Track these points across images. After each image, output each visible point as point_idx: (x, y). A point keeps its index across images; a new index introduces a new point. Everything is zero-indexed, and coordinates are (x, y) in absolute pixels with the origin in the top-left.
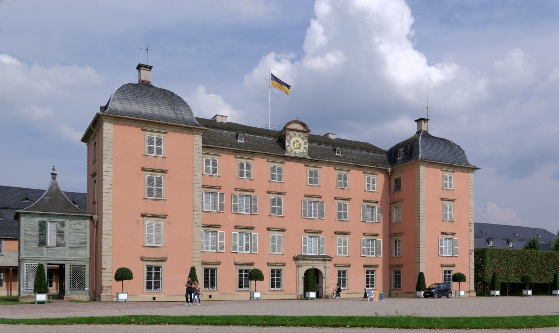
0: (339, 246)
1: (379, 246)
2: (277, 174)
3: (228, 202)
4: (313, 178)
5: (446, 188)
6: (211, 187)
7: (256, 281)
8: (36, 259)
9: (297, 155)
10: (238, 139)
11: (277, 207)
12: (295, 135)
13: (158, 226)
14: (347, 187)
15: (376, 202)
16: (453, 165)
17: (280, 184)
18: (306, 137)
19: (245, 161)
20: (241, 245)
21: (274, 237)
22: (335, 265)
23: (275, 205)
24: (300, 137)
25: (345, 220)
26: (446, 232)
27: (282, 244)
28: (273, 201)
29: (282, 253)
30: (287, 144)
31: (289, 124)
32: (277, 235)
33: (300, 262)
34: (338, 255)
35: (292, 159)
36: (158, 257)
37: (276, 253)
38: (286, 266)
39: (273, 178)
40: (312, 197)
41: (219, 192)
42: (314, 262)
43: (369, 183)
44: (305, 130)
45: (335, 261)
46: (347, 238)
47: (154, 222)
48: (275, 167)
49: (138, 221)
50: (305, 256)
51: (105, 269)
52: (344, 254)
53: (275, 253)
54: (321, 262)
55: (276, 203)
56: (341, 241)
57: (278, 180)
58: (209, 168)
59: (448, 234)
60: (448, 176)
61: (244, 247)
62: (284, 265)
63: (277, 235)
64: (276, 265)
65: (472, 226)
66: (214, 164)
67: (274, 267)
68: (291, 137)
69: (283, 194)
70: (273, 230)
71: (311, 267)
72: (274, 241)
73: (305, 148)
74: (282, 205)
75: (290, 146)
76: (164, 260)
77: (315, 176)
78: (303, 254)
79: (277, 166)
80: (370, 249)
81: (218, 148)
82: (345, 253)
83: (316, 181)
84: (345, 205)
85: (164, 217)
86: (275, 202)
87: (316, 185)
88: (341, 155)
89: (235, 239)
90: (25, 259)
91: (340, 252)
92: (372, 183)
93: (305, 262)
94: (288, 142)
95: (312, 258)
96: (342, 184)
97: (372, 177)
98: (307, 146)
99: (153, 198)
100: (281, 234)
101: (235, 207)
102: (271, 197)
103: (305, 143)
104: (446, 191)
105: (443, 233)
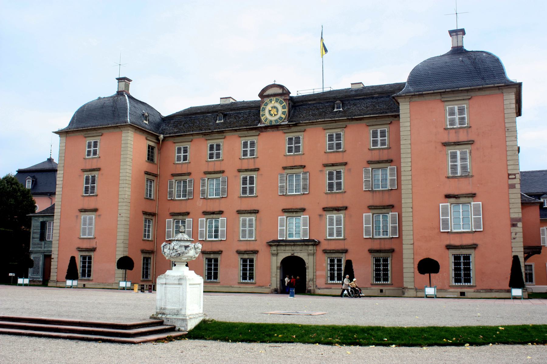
0: (329, 226)
2: (249, 149)
4: (293, 145)
5: (451, 127)
7: (431, 274)
8: (38, 251)
9: (274, 123)
10: (217, 120)
11: (249, 186)
13: (91, 219)
14: (340, 148)
16: (458, 90)
17: (253, 160)
18: (284, 100)
19: (214, 142)
21: (244, 221)
22: (325, 252)
23: (246, 185)
25: (338, 191)
26: (456, 192)
27: (254, 228)
28: (245, 179)
29: (253, 239)
31: (264, 90)
32: (248, 219)
33: (274, 248)
34: (328, 238)
35: (267, 129)
36: (89, 248)
37: (247, 239)
38: (259, 254)
40: (292, 169)
41: (188, 178)
42: (293, 248)
43: (377, 137)
44: (284, 92)
46: (342, 215)
47: (88, 216)
48: (247, 142)
49: (77, 216)
50: (283, 241)
51: (53, 259)
52: (337, 237)
53: (246, 239)
54: (304, 247)
55: (248, 182)
56: (333, 219)
57: (250, 155)
58: (181, 155)
59: (459, 197)
60: (456, 108)
61: (213, 234)
63: (248, 219)
65: (515, 178)
67: (244, 256)
68: (266, 104)
69: (257, 170)
70: (245, 213)
71: (290, 255)
72: (244, 225)
73: (283, 113)
74: (254, 183)
75: (264, 115)
76: (94, 250)
77: (296, 143)
79: (249, 140)
80: (381, 227)
81: (187, 134)
82: (339, 234)
83: (297, 149)
84: (339, 173)
85: (95, 210)
86: (247, 181)
87: (297, 153)
88: (341, 109)
90: (32, 251)
91: (331, 234)
92: (381, 137)
94: (262, 111)
95: (294, 243)
96: (333, 146)
99: (88, 195)
102: (242, 176)
103: (284, 107)
104: (454, 131)
105: (448, 196)
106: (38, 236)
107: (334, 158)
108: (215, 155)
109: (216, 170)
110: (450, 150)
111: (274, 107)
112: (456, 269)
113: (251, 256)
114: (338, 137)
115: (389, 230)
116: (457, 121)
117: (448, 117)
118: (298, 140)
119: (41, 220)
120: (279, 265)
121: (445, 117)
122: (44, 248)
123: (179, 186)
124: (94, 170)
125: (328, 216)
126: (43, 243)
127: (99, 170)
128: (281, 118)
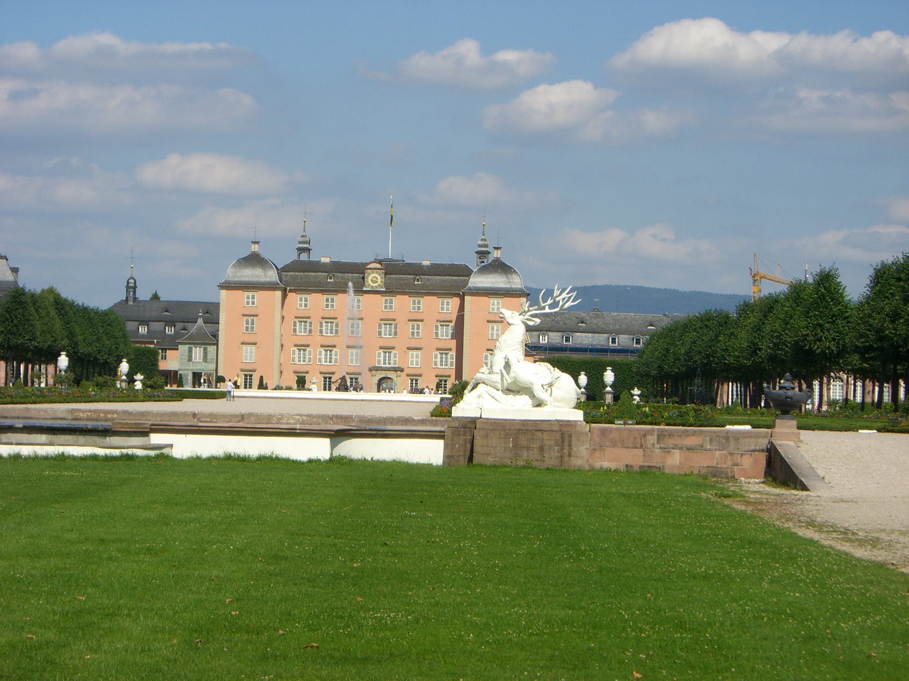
1: (452, 358)
3: (316, 327)
12: (373, 273)
15: (451, 321)
19: (330, 297)
20: (326, 358)
22: (408, 375)
33: (374, 372)
41: (309, 321)
42: (387, 372)
45: (406, 372)
46: (419, 352)
47: (249, 348)
60: (496, 301)
61: (328, 360)
62: (360, 374)
66: (306, 300)
68: (369, 274)
72: (352, 355)
73: (381, 282)
82: (417, 364)
83: (391, 307)
84: (418, 325)
85: (255, 344)
88: (420, 283)
89: (320, 354)
91: (412, 364)
93: (379, 372)
97: (445, 301)
98: (383, 280)
101: (321, 331)
103: (381, 278)
105: (487, 350)
106: (187, 358)
107: (415, 317)
110: (491, 325)
111: (374, 277)
113: (330, 376)
114: (419, 303)
115: (449, 363)
116: (496, 309)
118: (391, 302)
119: (187, 346)
121: (490, 306)
122: (193, 366)
125: (411, 352)
126: (191, 363)
127: (257, 316)
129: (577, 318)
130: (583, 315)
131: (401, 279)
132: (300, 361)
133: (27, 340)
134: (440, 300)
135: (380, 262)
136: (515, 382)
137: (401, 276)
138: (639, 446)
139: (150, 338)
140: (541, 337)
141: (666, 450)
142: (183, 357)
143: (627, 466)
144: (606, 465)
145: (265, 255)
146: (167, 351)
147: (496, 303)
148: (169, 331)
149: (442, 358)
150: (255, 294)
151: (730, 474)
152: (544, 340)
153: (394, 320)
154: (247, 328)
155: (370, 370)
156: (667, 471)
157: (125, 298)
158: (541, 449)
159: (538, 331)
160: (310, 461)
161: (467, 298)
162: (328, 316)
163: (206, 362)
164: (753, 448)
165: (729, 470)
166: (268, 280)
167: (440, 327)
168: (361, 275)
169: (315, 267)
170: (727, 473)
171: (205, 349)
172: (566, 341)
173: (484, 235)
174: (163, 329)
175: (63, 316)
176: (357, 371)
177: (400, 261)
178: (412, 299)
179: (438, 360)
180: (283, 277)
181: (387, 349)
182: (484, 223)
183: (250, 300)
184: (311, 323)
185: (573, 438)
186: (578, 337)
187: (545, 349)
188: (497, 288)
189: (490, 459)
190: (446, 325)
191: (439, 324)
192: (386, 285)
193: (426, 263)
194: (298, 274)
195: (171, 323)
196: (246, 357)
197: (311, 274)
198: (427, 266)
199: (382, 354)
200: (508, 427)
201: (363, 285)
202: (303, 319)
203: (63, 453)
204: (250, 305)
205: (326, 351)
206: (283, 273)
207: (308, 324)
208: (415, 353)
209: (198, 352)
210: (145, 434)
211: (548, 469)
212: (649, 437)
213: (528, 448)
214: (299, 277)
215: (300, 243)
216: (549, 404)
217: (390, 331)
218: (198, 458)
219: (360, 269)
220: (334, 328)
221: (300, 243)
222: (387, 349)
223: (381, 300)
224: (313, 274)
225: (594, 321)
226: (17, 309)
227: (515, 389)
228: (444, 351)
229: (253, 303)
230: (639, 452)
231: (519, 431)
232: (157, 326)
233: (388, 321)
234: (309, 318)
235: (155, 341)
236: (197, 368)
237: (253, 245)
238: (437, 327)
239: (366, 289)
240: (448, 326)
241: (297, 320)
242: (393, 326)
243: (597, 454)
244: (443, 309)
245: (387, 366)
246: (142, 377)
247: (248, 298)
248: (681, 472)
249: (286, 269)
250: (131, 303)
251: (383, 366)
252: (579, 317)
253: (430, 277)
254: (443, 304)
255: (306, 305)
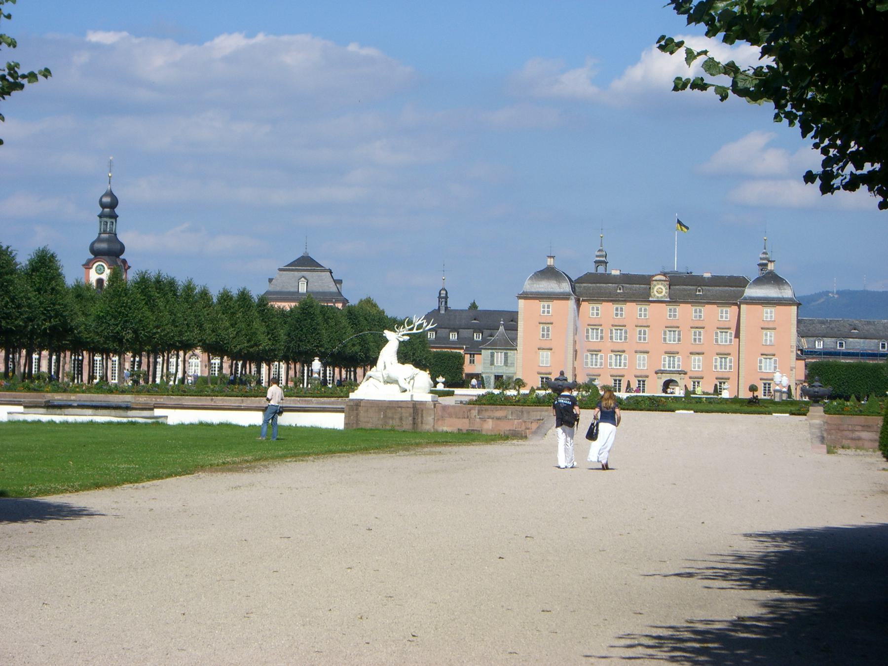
1: (731, 362)
2: (643, 313)
6: (595, 325)
12: (658, 284)
19: (619, 306)
20: (616, 362)
21: (640, 357)
22: (690, 378)
24: (662, 284)
26: (766, 353)
28: (640, 331)
30: (651, 291)
33: (660, 374)
37: (642, 368)
39: (640, 315)
41: (600, 328)
45: (689, 374)
46: (701, 357)
47: (545, 353)
49: (536, 352)
60: (769, 310)
62: (647, 377)
64: (641, 377)
66: (597, 309)
68: (655, 286)
69: (648, 326)
71: (669, 378)
73: (666, 292)
77: (674, 312)
78: (662, 369)
79: (643, 307)
82: (699, 367)
83: (675, 316)
84: (700, 332)
85: (551, 349)
88: (701, 293)
89: (611, 359)
91: (695, 368)
93: (664, 374)
97: (724, 309)
100: (646, 356)
101: (611, 338)
103: (666, 289)
105: (762, 355)
106: (489, 362)
108: (619, 315)
109: (620, 324)
110: (765, 332)
111: (660, 288)
112: (764, 390)
113: (620, 378)
114: (700, 311)
116: (769, 317)
117: (765, 315)
118: (675, 311)
119: (490, 351)
120: (662, 384)
123: (593, 332)
124: (548, 324)
125: (693, 357)
126: (493, 367)
127: (552, 323)
128: (664, 295)
129: (851, 325)
130: (857, 322)
131: (685, 290)
132: (592, 365)
133: (315, 346)
134: (720, 309)
135: (665, 274)
136: (388, 377)
137: (684, 287)
138: (466, 417)
139: (460, 344)
140: (817, 342)
141: (483, 420)
142: (487, 362)
143: (459, 429)
144: (445, 429)
145: (559, 267)
146: (475, 355)
147: (769, 312)
148: (477, 337)
149: (721, 362)
150: (550, 304)
151: (523, 435)
152: (819, 345)
153: (678, 327)
154: (543, 335)
155: (656, 373)
156: (484, 433)
157: (437, 308)
158: (401, 419)
159: (814, 337)
160: (250, 426)
161: (743, 307)
162: (617, 324)
163: (507, 366)
164: (539, 418)
165: (523, 433)
166: (562, 290)
167: (719, 334)
168: (648, 287)
169: (607, 279)
170: (522, 434)
171: (506, 354)
172: (840, 346)
173: (765, 249)
174: (471, 336)
175: (356, 326)
176: (644, 374)
177: (685, 273)
178: (694, 308)
179: (718, 364)
180: (577, 288)
181: (671, 353)
182: (765, 238)
183: (546, 310)
184: (602, 330)
185: (424, 412)
186: (851, 342)
187: (820, 354)
188: (770, 298)
189: (369, 425)
190: (725, 332)
191: (718, 331)
192: (670, 296)
193: (707, 275)
194: (590, 285)
195: (479, 330)
196: (543, 361)
197: (601, 285)
198: (708, 278)
199: (667, 359)
200: (380, 405)
201: (649, 295)
202: (595, 326)
203: (92, 420)
204: (546, 314)
205: (616, 355)
206: (577, 285)
207: (599, 331)
208: (697, 357)
209: (499, 357)
210: (152, 409)
211: (404, 431)
212: (472, 411)
213: (393, 418)
214: (591, 288)
215: (597, 256)
216: (408, 390)
217: (674, 337)
218: (183, 424)
219: (647, 280)
220: (623, 335)
221: (597, 256)
222: (671, 353)
223: (665, 309)
224: (605, 285)
225: (866, 328)
226: (306, 320)
227: (390, 381)
228: (724, 355)
229: (548, 312)
230: (467, 421)
231: (388, 407)
232: (465, 333)
233: (672, 328)
234: (601, 325)
235: (464, 347)
236: (499, 372)
237: (549, 260)
238: (717, 333)
239: (652, 299)
240: (727, 332)
241: (589, 328)
242: (677, 332)
243: (440, 422)
244: (722, 317)
245: (671, 369)
246: (444, 379)
247: (544, 307)
248: (493, 434)
249: (580, 280)
250: (443, 312)
251: (668, 369)
252: (852, 324)
253: (711, 288)
254: (722, 313)
255: (597, 314)
